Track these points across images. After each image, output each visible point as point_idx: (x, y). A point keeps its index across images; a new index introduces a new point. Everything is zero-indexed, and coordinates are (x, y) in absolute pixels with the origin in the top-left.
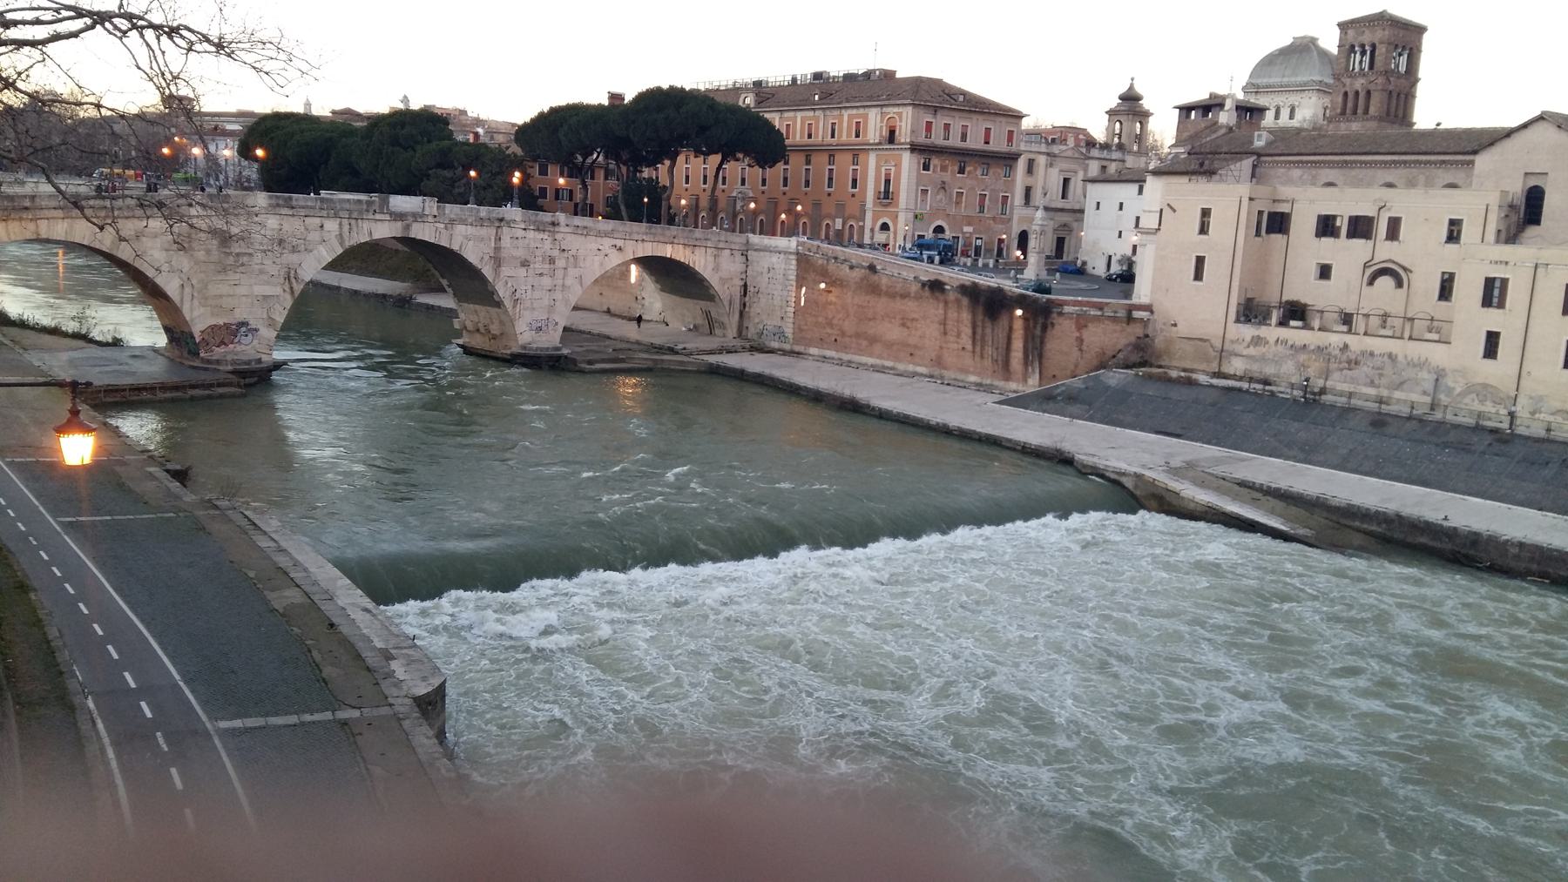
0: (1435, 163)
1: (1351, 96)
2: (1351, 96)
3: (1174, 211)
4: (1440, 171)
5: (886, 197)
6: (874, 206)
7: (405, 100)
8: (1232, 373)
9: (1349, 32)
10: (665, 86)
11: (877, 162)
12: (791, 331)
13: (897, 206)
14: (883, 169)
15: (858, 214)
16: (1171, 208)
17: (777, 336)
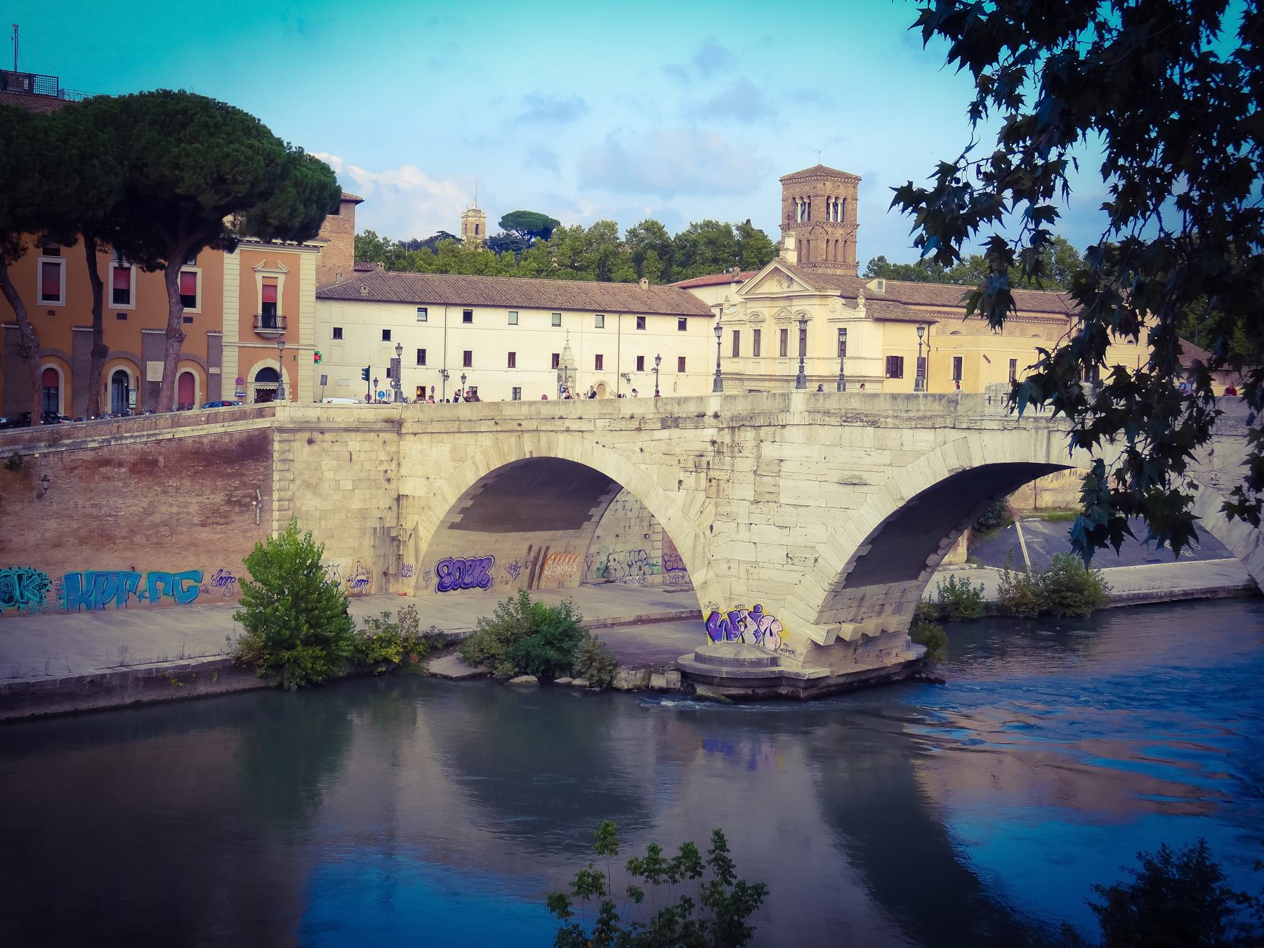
0: (1048, 319)
1: (832, 243)
2: (832, 243)
3: (989, 362)
4: (1029, 324)
5: (266, 324)
6: (242, 337)
7: (910, 183)
8: (1044, 507)
9: (827, 183)
10: (136, 93)
11: (242, 264)
12: (659, 553)
13: (297, 341)
14: (259, 277)
15: (202, 353)
16: (987, 359)
17: (635, 569)
